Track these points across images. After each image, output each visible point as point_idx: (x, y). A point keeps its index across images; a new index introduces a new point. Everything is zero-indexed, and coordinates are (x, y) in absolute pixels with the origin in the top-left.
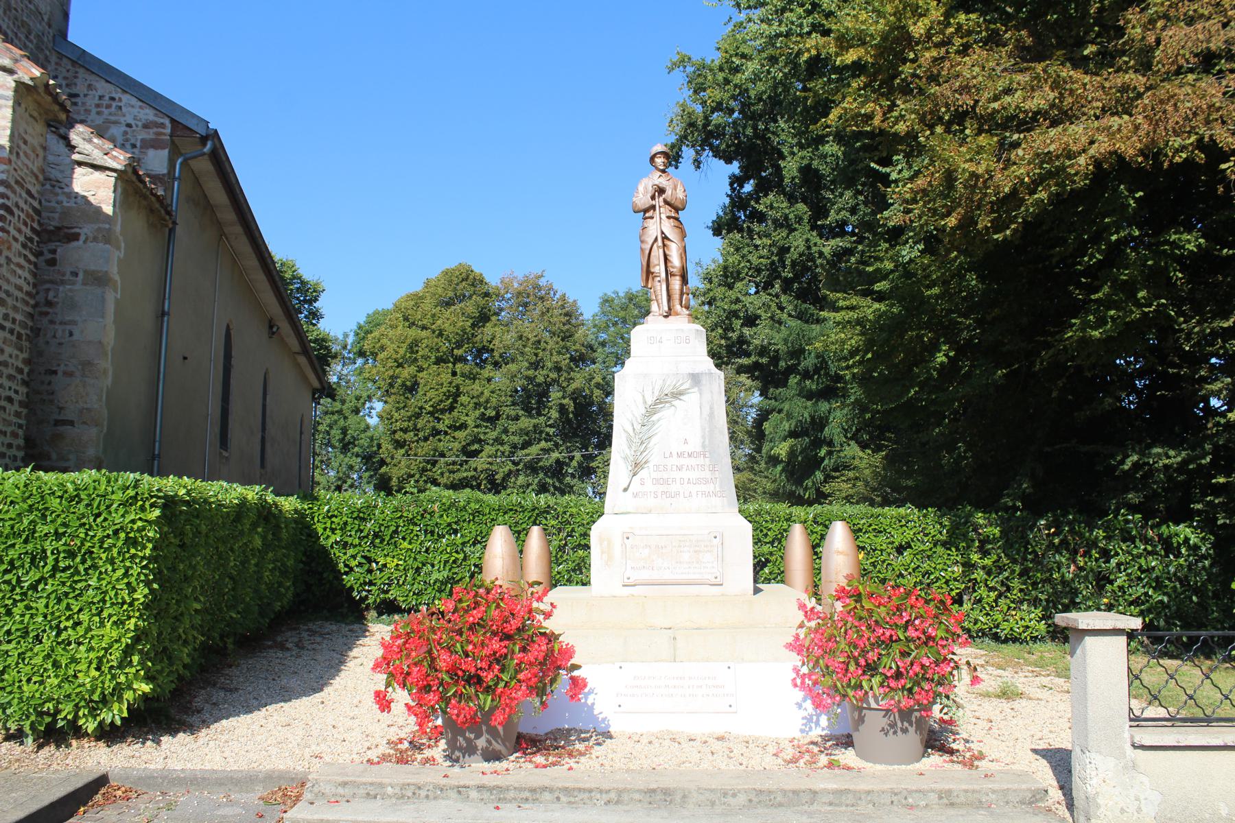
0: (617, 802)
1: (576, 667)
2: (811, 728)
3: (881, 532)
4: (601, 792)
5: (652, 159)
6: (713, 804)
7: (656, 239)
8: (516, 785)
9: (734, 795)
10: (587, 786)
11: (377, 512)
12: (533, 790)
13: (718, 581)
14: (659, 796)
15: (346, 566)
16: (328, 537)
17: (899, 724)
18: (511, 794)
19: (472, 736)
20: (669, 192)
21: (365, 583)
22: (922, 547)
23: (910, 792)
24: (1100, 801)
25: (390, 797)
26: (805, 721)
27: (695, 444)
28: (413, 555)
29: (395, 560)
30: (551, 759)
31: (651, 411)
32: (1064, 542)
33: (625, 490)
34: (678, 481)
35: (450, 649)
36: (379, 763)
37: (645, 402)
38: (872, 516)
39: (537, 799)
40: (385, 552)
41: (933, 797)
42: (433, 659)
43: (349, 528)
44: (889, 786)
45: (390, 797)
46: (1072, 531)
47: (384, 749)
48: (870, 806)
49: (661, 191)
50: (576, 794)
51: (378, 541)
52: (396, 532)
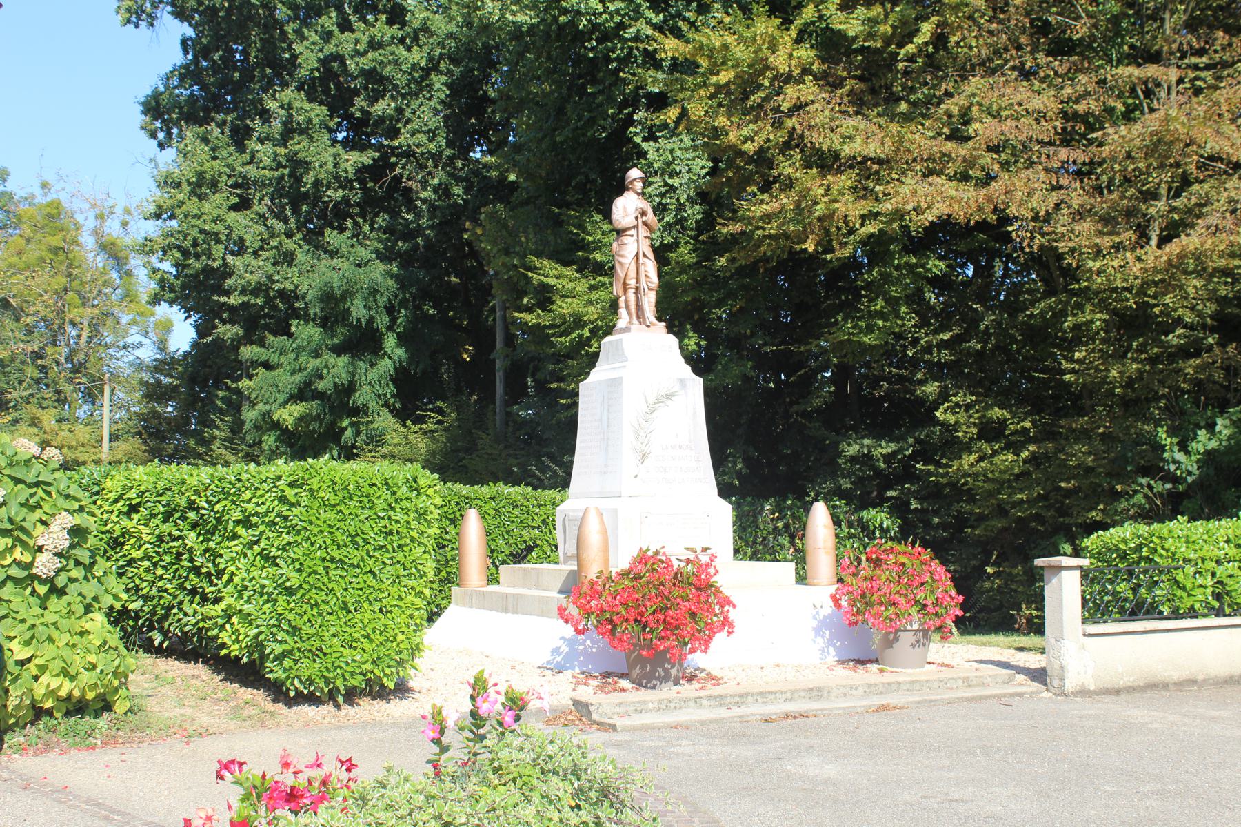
0: (792, 699)
10: (773, 689)
12: (741, 696)
14: (815, 693)
18: (728, 700)
32: (786, 526)
41: (960, 681)
46: (793, 516)
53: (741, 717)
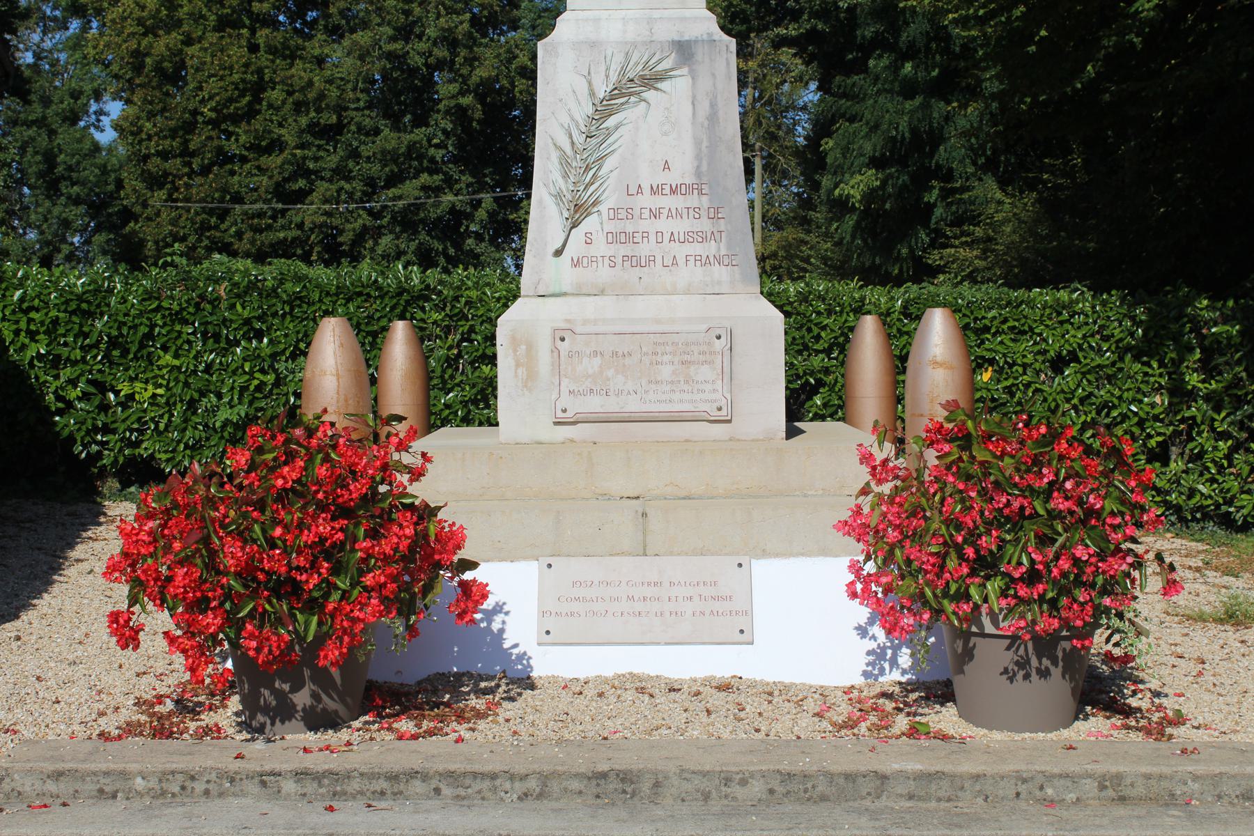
0: (540, 796)
3: (1023, 333)
4: (512, 777)
6: (706, 797)
8: (364, 769)
9: (743, 782)
10: (488, 768)
12: (393, 777)
14: (613, 785)
15: (59, 398)
16: (24, 347)
17: (1034, 662)
18: (355, 785)
19: (286, 687)
21: (96, 430)
22: (1098, 361)
23: (1050, 777)
25: (140, 794)
26: (871, 658)
27: (682, 171)
28: (182, 377)
29: (150, 387)
30: (426, 724)
31: (604, 109)
33: (558, 253)
34: (652, 238)
35: (243, 536)
36: (120, 737)
37: (592, 94)
38: (1009, 303)
39: (401, 793)
41: (1090, 786)
42: (213, 554)
43: (61, 331)
44: (1012, 767)
45: (140, 794)
47: (129, 713)
48: (980, 800)
50: (468, 782)
51: (116, 353)
52: (149, 336)
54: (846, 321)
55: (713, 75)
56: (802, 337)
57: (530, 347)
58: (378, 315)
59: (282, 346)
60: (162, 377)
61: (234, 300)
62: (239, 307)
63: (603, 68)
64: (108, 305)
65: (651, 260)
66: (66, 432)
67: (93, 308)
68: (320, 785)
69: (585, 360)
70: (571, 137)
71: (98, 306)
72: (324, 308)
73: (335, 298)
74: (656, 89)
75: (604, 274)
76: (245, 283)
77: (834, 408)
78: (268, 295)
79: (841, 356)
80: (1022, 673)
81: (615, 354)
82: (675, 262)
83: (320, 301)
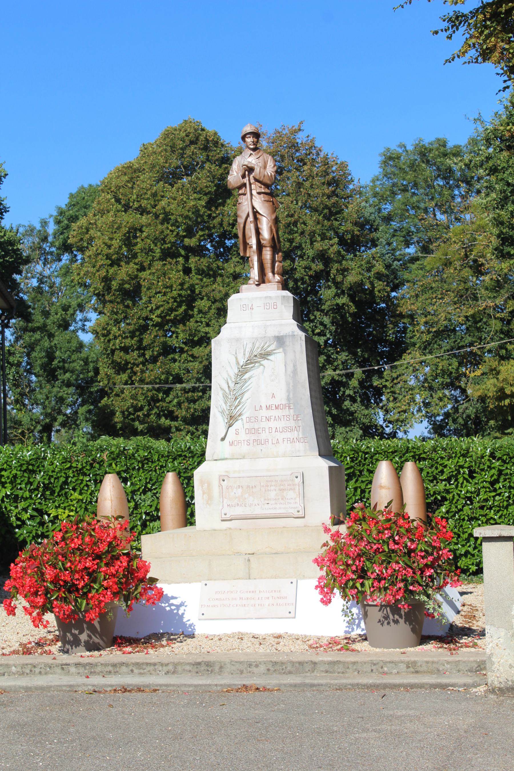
0: (174, 673)
1: (153, 580)
2: (353, 629)
4: (162, 665)
5: (244, 138)
6: (242, 672)
7: (248, 215)
9: (257, 666)
10: (152, 661)
11: (46, 463)
12: (114, 665)
13: (301, 514)
14: (203, 668)
15: (18, 519)
17: (391, 617)
18: (99, 669)
19: (77, 632)
20: (257, 170)
21: (37, 536)
23: (386, 663)
24: (494, 659)
25: (14, 674)
27: (281, 398)
28: (83, 506)
29: (67, 511)
30: (136, 650)
31: (243, 370)
33: (223, 439)
34: (267, 430)
35: (54, 566)
36: (9, 655)
37: (238, 363)
39: (117, 672)
40: (56, 504)
41: (403, 666)
42: (43, 574)
43: (19, 481)
44: (369, 659)
45: (14, 674)
47: (16, 646)
48: (356, 673)
49: (250, 170)
50: (144, 667)
51: (48, 493)
52: (66, 483)
53: (71, 686)
54: (458, 462)
55: (294, 352)
56: (432, 472)
57: (209, 485)
58: (190, 467)
59: (138, 487)
60: (73, 506)
61: (111, 462)
62: (114, 465)
63: (242, 351)
64: (43, 466)
65: (266, 441)
66: (21, 538)
67: (35, 468)
68: (85, 669)
69: (235, 490)
70: (228, 384)
71: (38, 467)
72: (160, 464)
73: (167, 458)
74: (268, 359)
75: (244, 449)
76: (117, 452)
77: (452, 514)
78: (130, 458)
79: (456, 483)
80: (386, 622)
81: (248, 487)
82: (278, 442)
83: (158, 460)
